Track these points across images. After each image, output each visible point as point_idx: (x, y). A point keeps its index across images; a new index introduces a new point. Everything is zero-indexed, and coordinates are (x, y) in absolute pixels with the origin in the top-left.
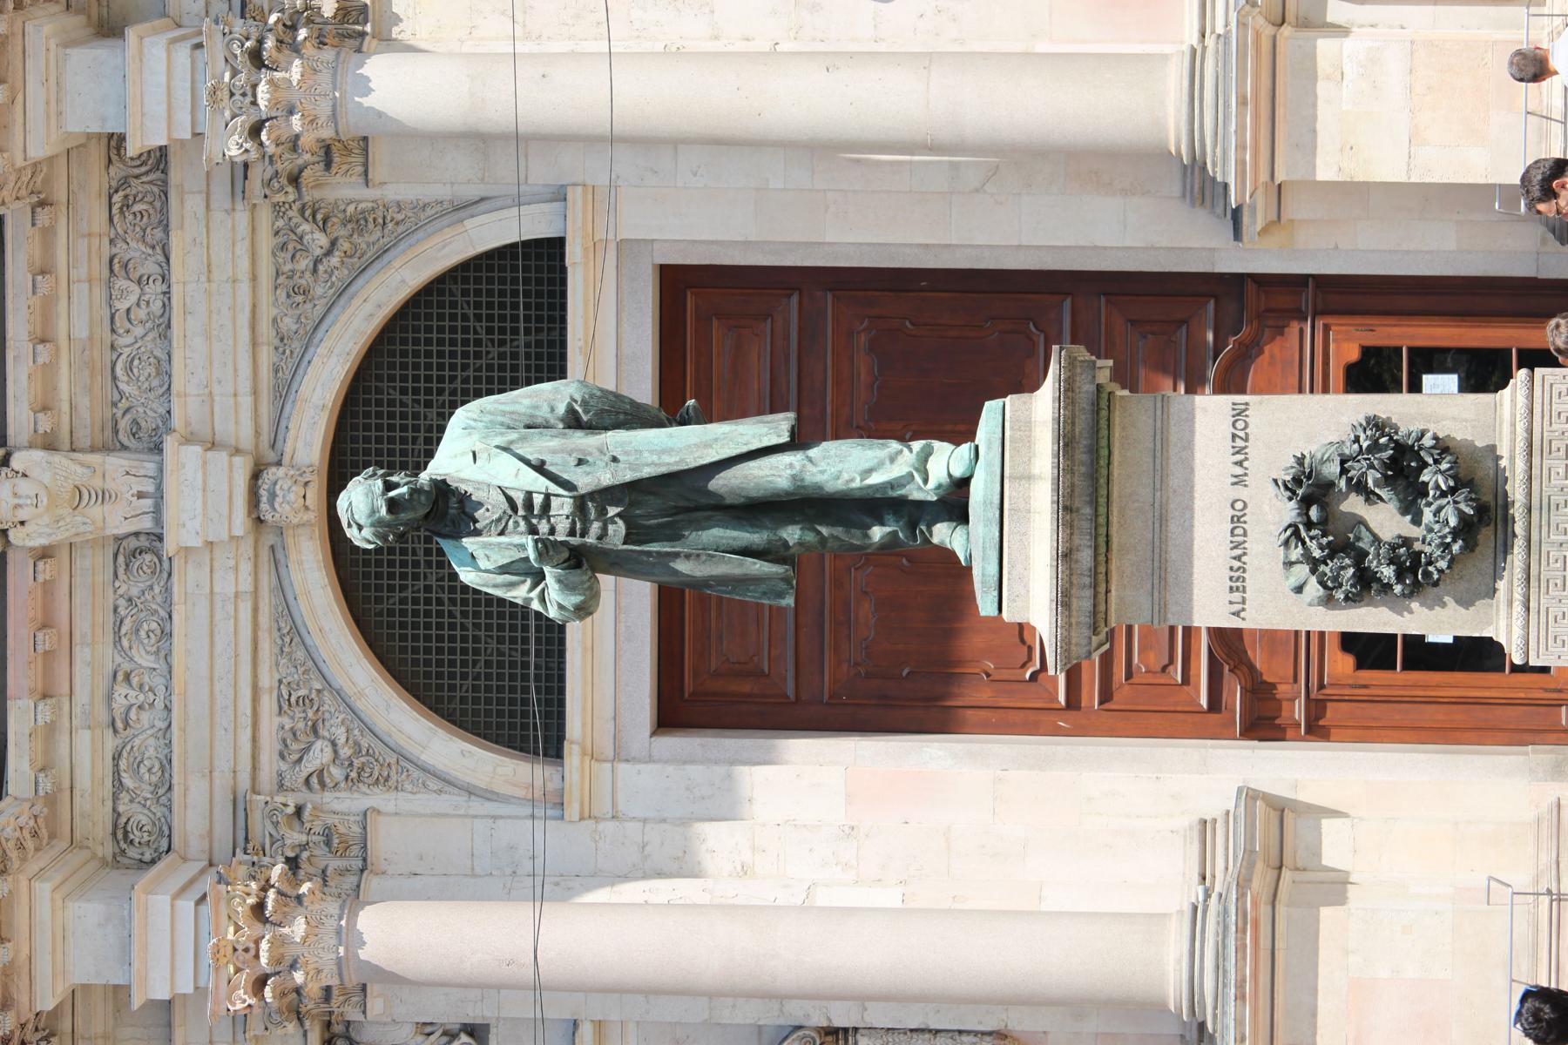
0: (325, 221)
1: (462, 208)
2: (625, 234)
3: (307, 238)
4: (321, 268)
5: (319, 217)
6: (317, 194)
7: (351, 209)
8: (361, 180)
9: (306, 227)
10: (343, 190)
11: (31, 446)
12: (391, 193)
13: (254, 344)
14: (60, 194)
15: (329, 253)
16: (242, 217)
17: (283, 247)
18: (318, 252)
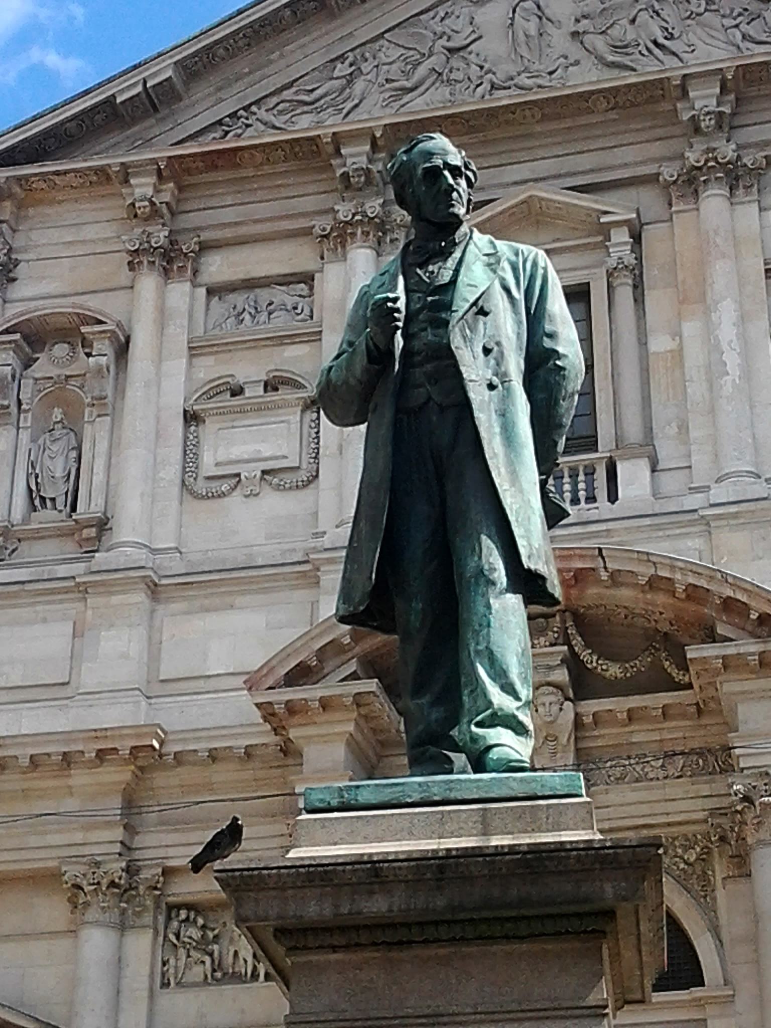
0: (703, 860)
1: (715, 931)
2: (709, 1022)
3: (692, 851)
4: (677, 859)
5: (704, 856)
6: (716, 855)
7: (710, 873)
8: (725, 875)
9: (698, 849)
10: (720, 869)
11: (577, 714)
12: (720, 894)
13: (636, 827)
14: (704, 721)
15: (686, 863)
16: (701, 815)
17: (687, 840)
18: (686, 857)
